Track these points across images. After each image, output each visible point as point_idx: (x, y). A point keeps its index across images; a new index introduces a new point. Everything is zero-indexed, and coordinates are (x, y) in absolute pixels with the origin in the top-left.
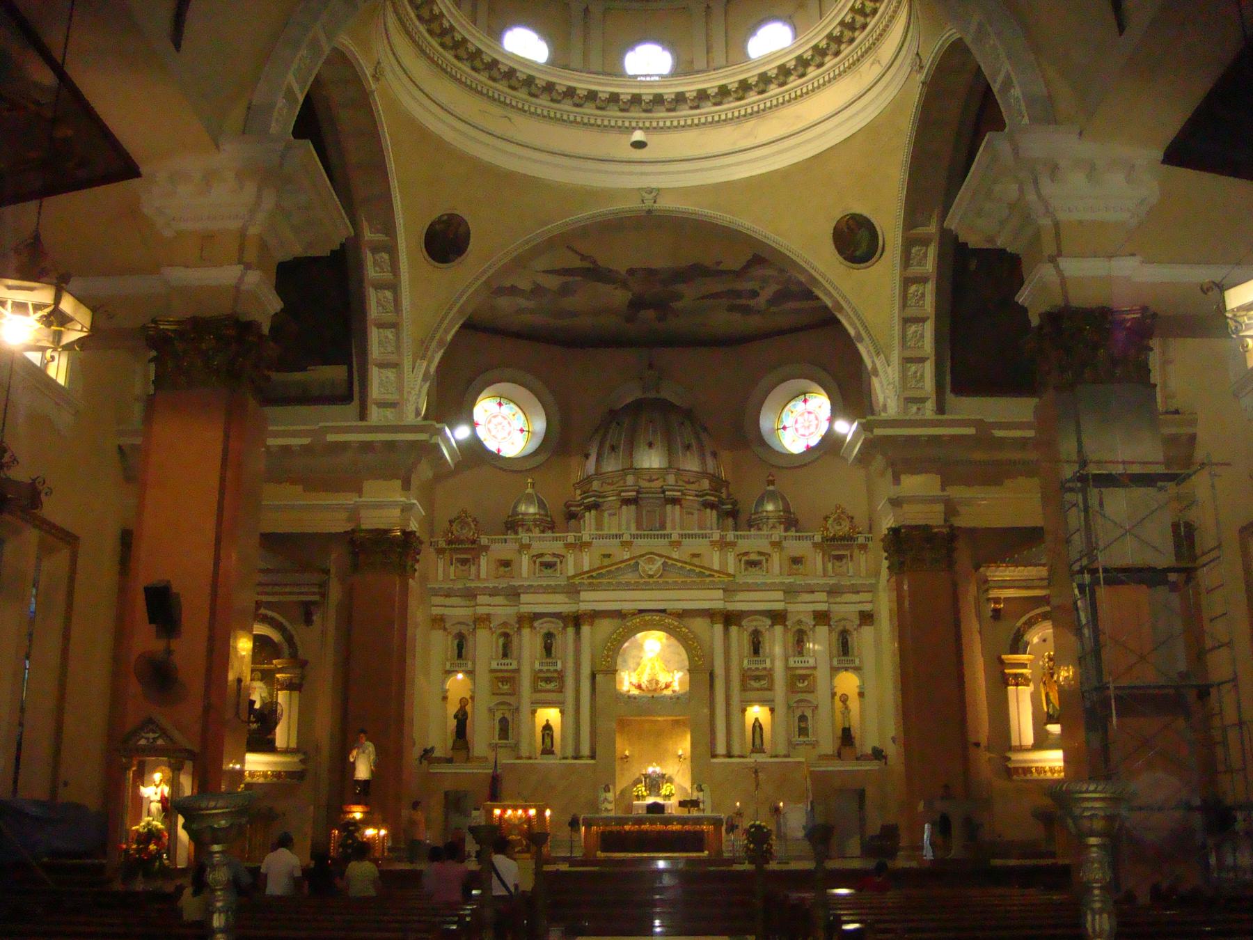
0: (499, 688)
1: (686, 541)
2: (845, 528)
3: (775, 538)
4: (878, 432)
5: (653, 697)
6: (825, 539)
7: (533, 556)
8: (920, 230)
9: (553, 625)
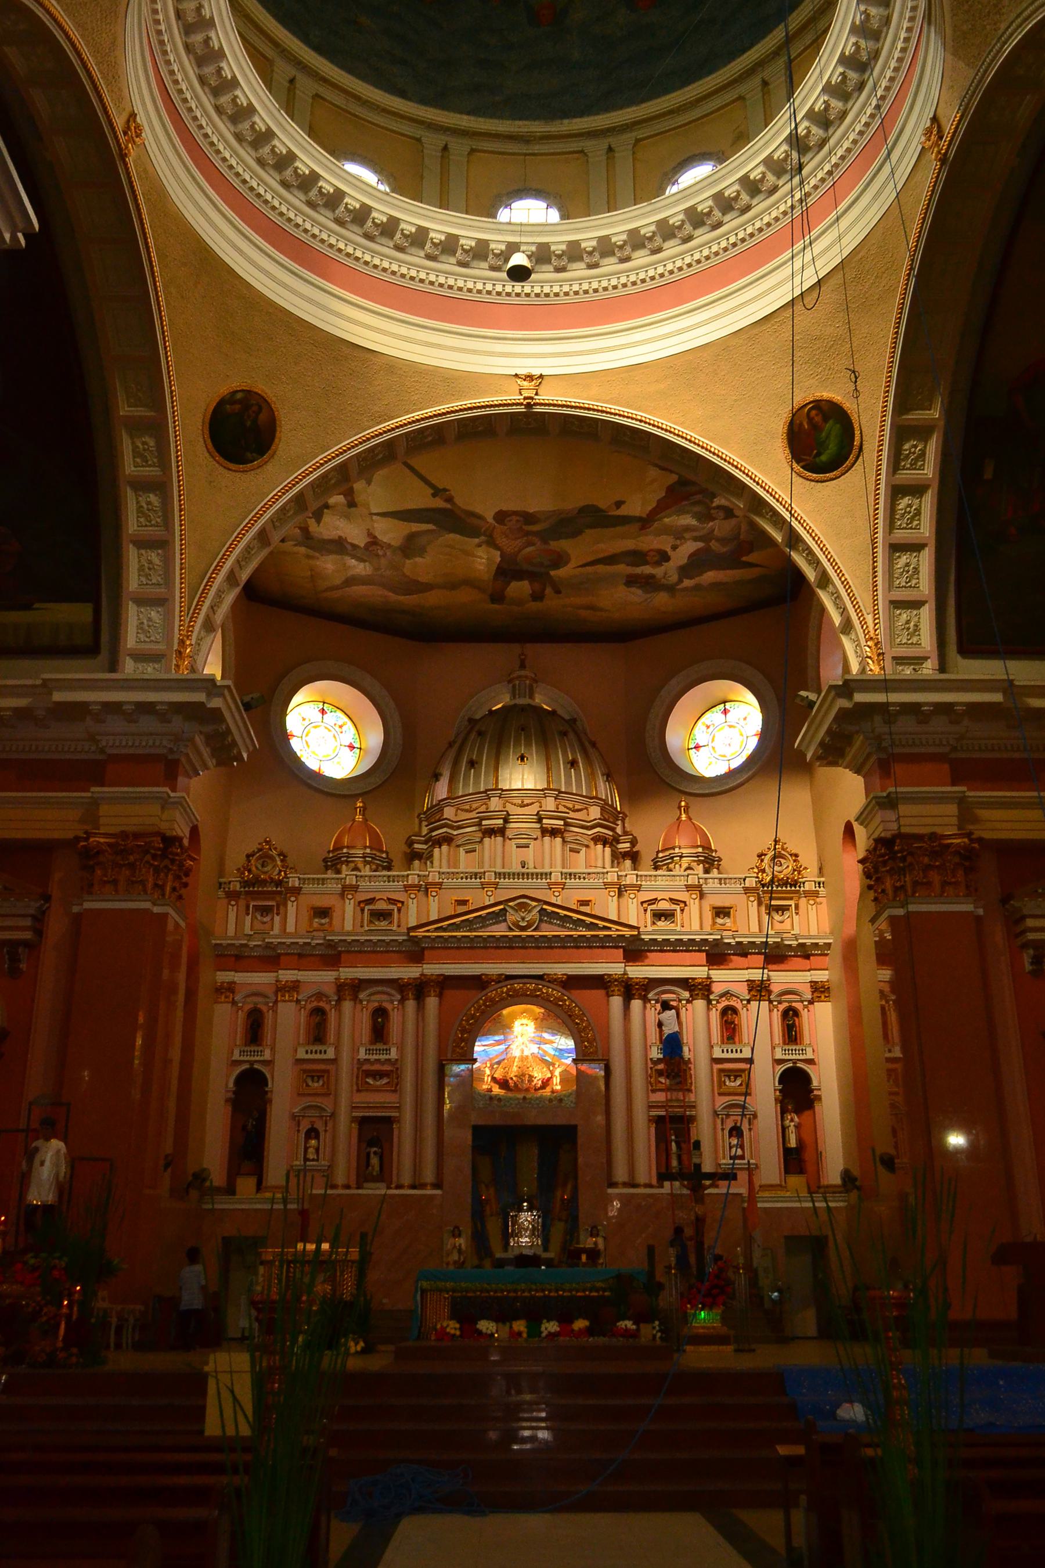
0: (307, 1085)
2: (785, 869)
3: (692, 880)
5: (524, 1098)
7: (360, 902)
8: (916, 416)
9: (384, 997)
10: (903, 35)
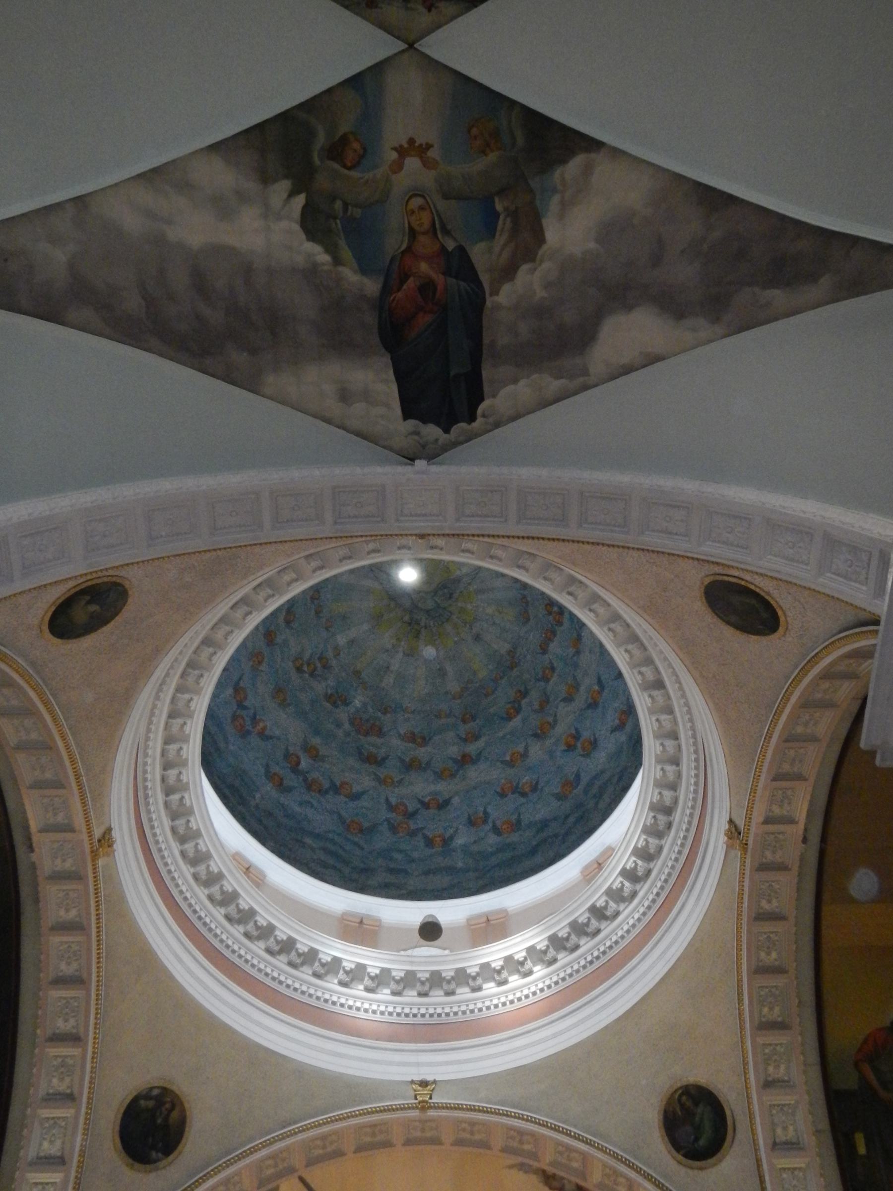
10: (693, 781)
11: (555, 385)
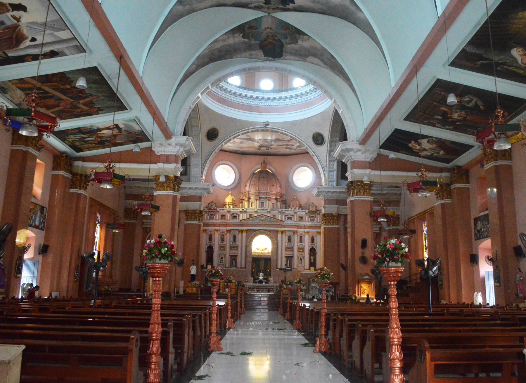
1: (272, 211)
2: (314, 209)
4: (321, 190)
6: (309, 212)
11: (298, 59)
